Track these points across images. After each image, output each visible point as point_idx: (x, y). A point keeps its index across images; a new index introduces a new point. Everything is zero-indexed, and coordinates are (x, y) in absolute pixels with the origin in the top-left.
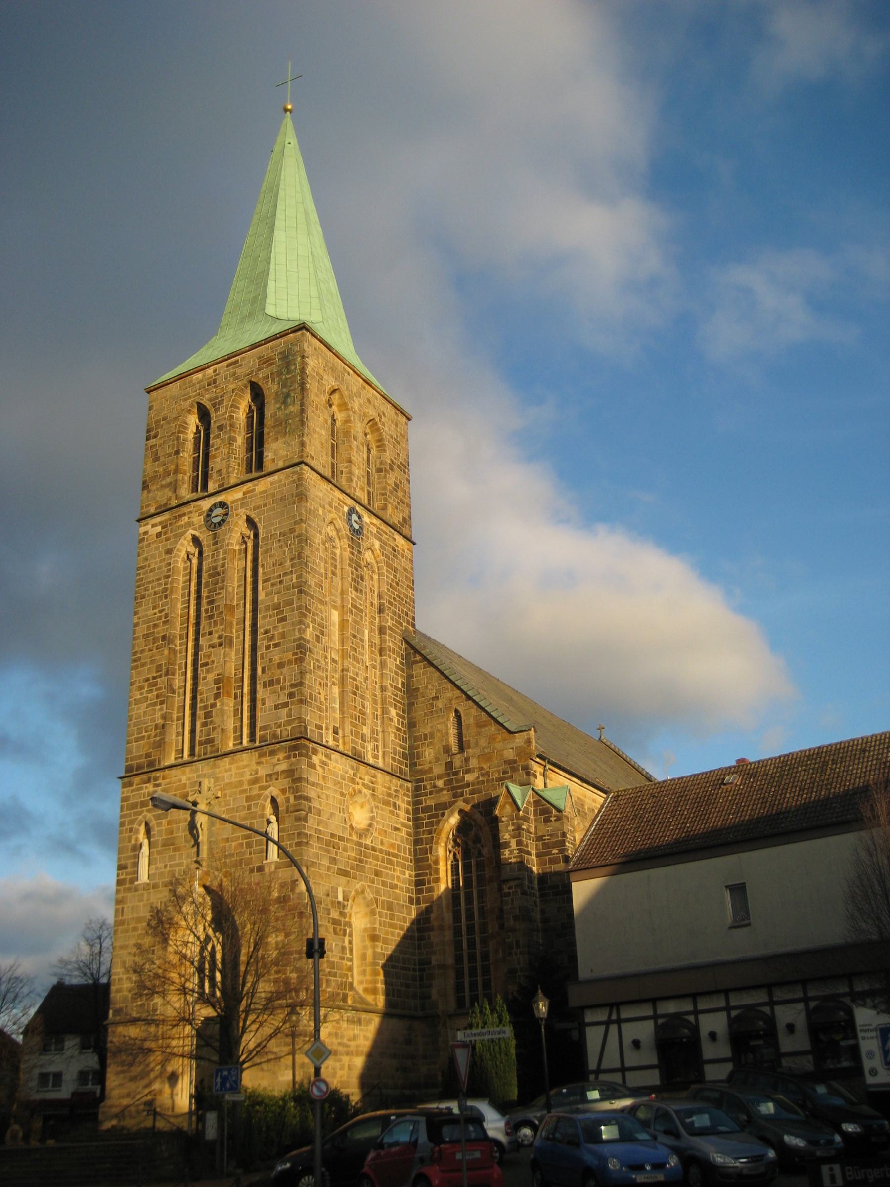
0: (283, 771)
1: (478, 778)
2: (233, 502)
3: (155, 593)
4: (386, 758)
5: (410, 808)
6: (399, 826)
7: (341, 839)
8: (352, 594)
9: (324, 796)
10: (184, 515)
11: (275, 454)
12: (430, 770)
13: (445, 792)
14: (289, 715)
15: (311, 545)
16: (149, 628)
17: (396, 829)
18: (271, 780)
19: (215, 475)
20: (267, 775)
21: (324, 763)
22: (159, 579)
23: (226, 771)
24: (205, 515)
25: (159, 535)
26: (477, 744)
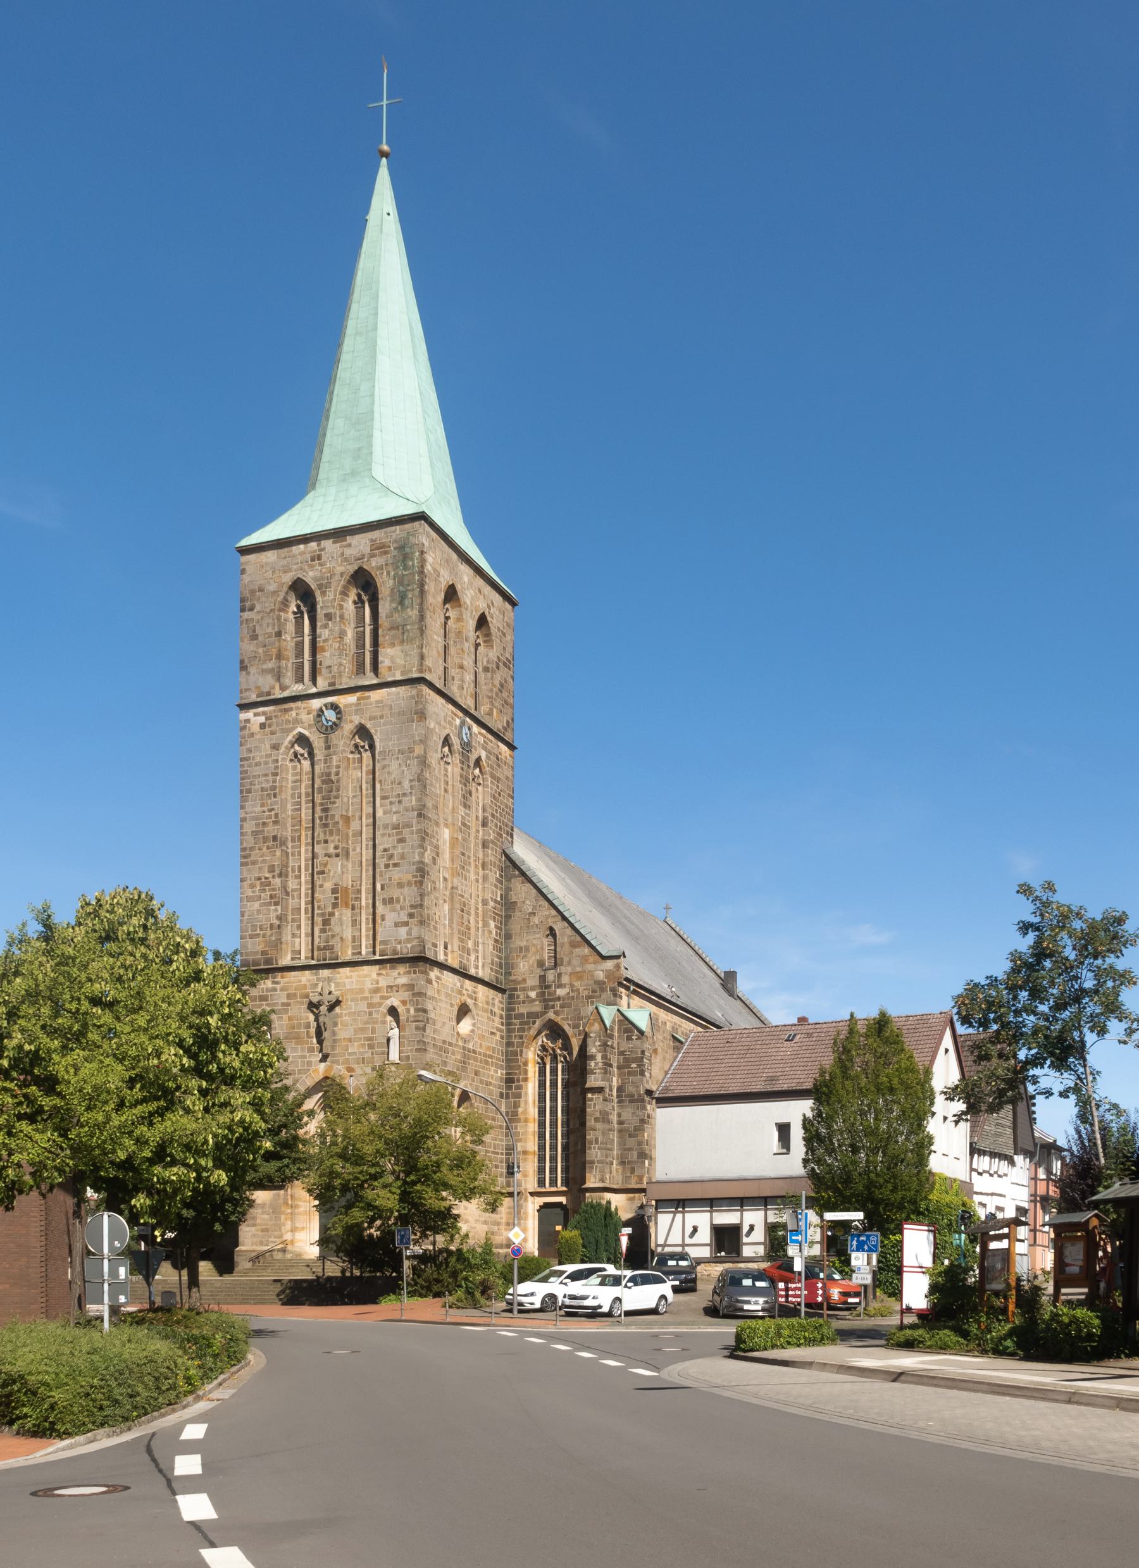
0: (404, 985)
1: (568, 993)
2: (346, 706)
3: (263, 789)
4: (486, 969)
5: (504, 1013)
6: (494, 1031)
7: (450, 1044)
8: (462, 811)
9: (438, 1008)
10: (291, 709)
11: (392, 662)
12: (524, 980)
13: (537, 1003)
14: (409, 933)
15: (429, 766)
16: (257, 825)
17: (492, 1033)
18: (392, 991)
19: (324, 671)
20: (387, 987)
21: (438, 978)
22: (266, 775)
23: (347, 977)
24: (315, 713)
25: (263, 726)
26: (569, 963)
